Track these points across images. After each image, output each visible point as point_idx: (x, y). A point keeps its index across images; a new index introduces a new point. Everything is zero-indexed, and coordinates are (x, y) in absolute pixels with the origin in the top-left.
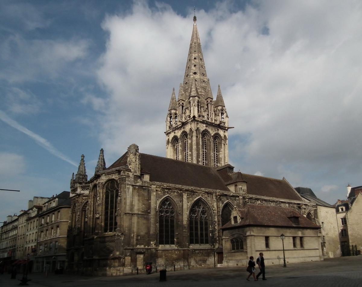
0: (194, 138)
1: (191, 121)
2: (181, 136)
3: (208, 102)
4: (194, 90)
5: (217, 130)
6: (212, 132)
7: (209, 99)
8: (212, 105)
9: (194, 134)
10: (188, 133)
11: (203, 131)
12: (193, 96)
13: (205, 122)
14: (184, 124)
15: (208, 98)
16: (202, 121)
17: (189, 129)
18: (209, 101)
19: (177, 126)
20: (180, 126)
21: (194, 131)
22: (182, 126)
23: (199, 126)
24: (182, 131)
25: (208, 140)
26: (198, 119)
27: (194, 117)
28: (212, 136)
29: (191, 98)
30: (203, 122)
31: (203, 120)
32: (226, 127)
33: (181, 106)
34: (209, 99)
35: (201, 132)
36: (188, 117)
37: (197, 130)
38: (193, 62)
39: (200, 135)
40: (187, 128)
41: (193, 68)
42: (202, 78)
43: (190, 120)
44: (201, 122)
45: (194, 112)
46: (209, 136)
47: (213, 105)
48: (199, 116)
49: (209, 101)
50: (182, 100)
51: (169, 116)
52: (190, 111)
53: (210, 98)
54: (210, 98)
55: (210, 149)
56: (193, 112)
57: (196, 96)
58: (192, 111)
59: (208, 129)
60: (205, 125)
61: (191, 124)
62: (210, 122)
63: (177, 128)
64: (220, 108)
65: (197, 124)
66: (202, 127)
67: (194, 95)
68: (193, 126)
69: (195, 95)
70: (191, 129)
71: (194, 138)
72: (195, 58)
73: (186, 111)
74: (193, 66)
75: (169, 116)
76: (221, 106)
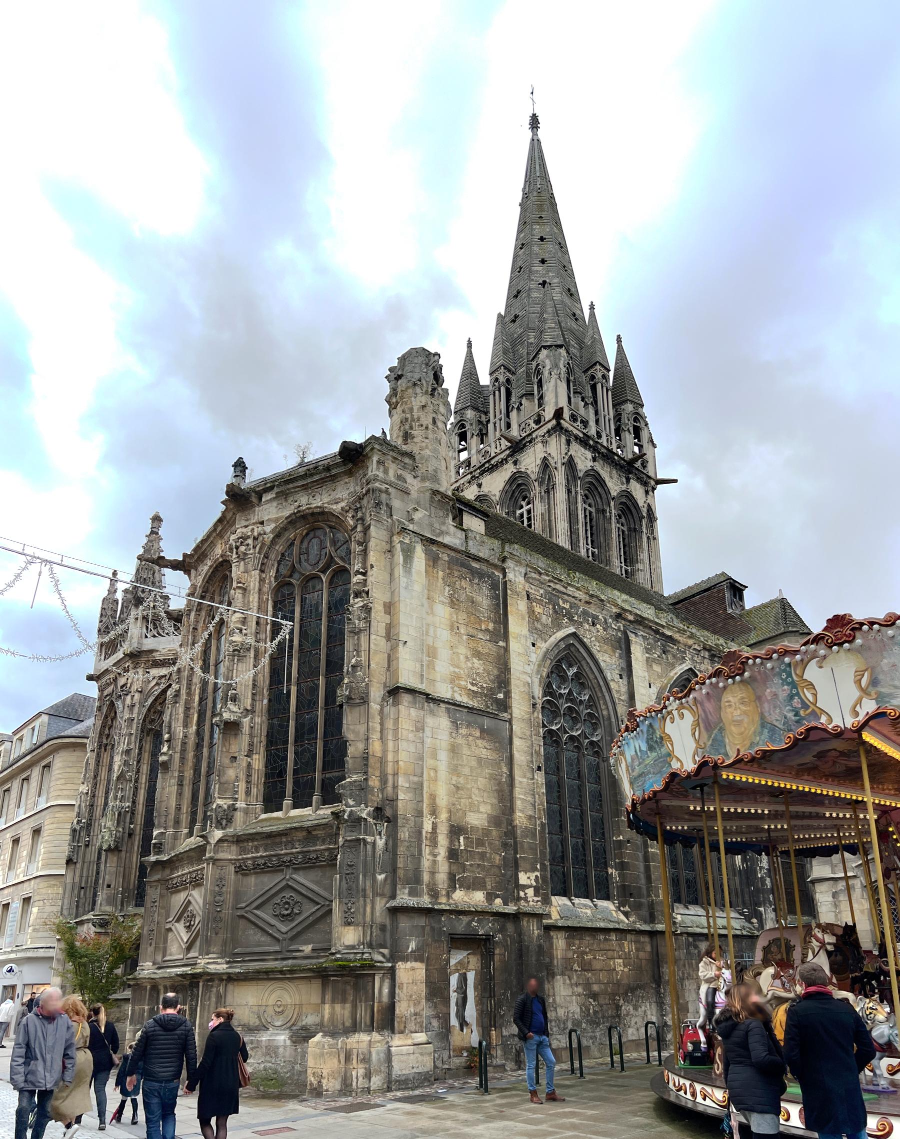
0: (560, 494)
1: (548, 432)
2: (504, 492)
3: (593, 377)
4: (553, 325)
5: (625, 481)
6: (614, 484)
7: (598, 367)
8: (607, 391)
9: (560, 478)
10: (533, 477)
11: (587, 474)
12: (550, 347)
13: (591, 442)
14: (517, 447)
15: (595, 364)
16: (581, 435)
17: (539, 462)
18: (599, 375)
19: (489, 461)
20: (502, 456)
21: (560, 468)
22: (509, 456)
23: (572, 452)
24: (509, 475)
25: (598, 511)
26: (571, 428)
27: (559, 414)
28: (613, 499)
29: (544, 352)
30: (584, 441)
31: (584, 433)
32: (650, 478)
33: (503, 389)
34: (598, 367)
35: (581, 475)
36: (531, 422)
37: (570, 464)
38: (536, 249)
39: (576, 486)
40: (530, 461)
41: (539, 268)
42: (567, 300)
43: (544, 430)
44: (577, 438)
45: (557, 397)
46: (604, 496)
47: (610, 393)
48: (574, 418)
49: (600, 375)
50: (505, 368)
51: (456, 431)
52: (541, 398)
53: (600, 364)
54: (600, 364)
55: (608, 546)
56: (554, 400)
57: (560, 346)
58: (549, 398)
59: (598, 466)
60: (589, 455)
61: (545, 443)
62: (605, 444)
63: (489, 468)
64: (629, 407)
65: (568, 442)
66: (584, 460)
67: (555, 343)
68: (556, 449)
69: (559, 343)
70: (545, 464)
71: (560, 494)
72: (542, 239)
73: (521, 404)
74: (537, 261)
75: (456, 431)
76: (632, 402)
